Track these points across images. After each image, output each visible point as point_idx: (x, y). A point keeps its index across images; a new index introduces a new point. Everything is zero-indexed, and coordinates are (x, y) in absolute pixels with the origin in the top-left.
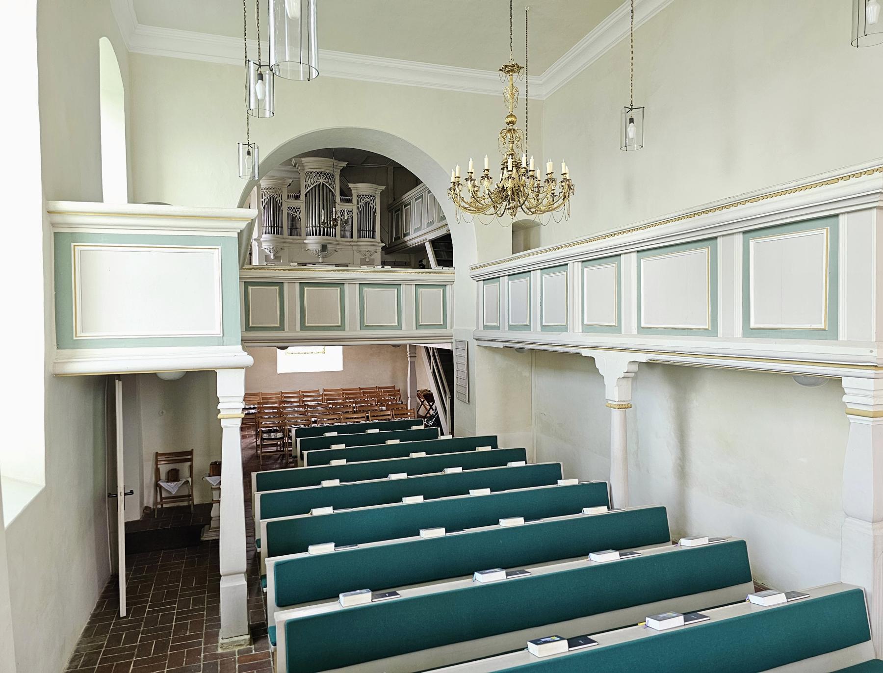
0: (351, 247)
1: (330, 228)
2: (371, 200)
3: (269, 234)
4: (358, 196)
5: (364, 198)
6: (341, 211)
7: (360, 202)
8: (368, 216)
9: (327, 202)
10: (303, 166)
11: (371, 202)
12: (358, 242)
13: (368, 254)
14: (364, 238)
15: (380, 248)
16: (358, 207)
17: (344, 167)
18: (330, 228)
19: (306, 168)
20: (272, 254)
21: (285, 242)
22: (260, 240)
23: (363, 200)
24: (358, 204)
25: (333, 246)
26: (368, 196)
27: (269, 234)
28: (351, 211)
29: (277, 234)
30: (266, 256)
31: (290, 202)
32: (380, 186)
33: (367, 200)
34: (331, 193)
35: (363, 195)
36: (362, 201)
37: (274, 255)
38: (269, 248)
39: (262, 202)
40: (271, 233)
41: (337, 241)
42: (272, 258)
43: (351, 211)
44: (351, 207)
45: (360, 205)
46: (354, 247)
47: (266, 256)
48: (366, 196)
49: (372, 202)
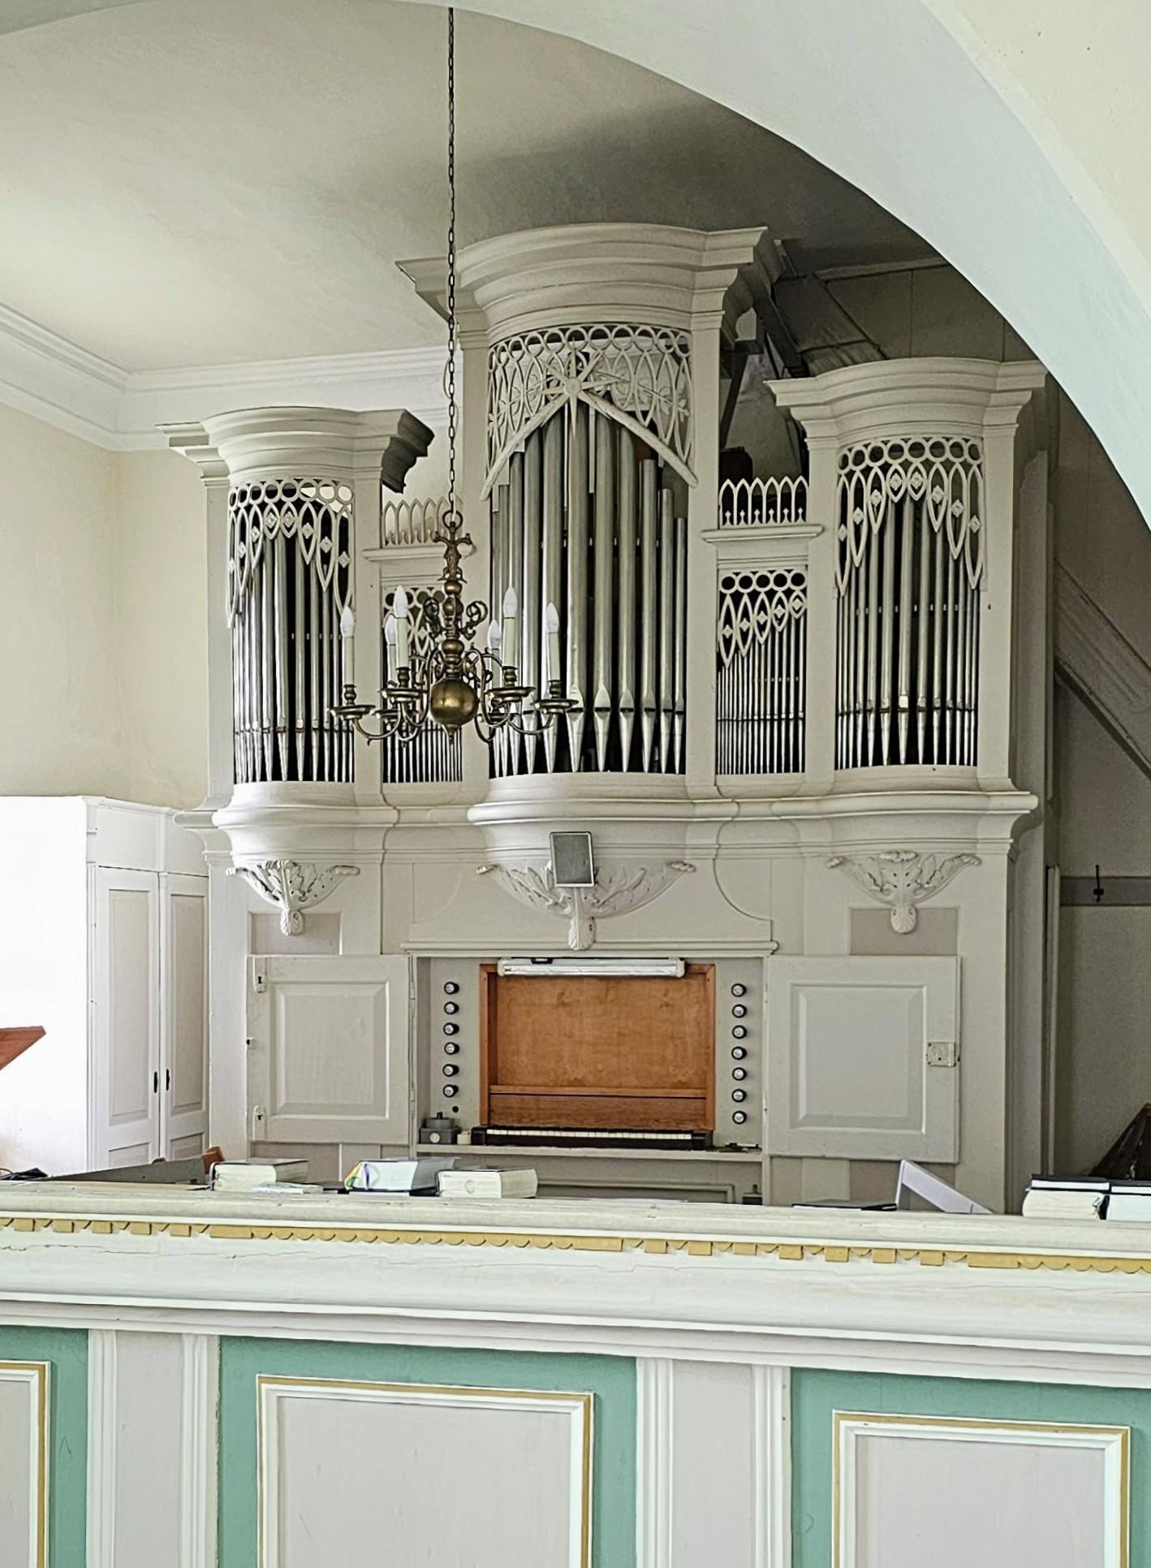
0: (783, 835)
1: (656, 712)
2: (938, 481)
3: (277, 776)
4: (844, 462)
5: (885, 468)
6: (728, 583)
7: (859, 503)
8: (915, 600)
9: (616, 533)
10: (479, 310)
11: (937, 494)
12: (832, 793)
13: (900, 881)
14: (878, 761)
15: (1005, 831)
16: (843, 545)
17: (740, 267)
18: (656, 712)
19: (495, 313)
20: (283, 906)
21: (353, 828)
22: (209, 819)
23: (877, 485)
24: (844, 520)
25: (662, 836)
26: (917, 449)
27: (264, 778)
28: (798, 579)
29: (308, 776)
30: (254, 916)
31: (389, 562)
32: (1005, 369)
33: (907, 482)
34: (648, 465)
35: (876, 454)
36: (870, 498)
37: (296, 913)
38: (258, 871)
39: (232, 575)
40: (277, 776)
41: (688, 799)
42: (284, 924)
43: (798, 579)
44: (796, 549)
45: (858, 528)
46: (807, 834)
47: (254, 916)
48: (896, 450)
49: (943, 494)
